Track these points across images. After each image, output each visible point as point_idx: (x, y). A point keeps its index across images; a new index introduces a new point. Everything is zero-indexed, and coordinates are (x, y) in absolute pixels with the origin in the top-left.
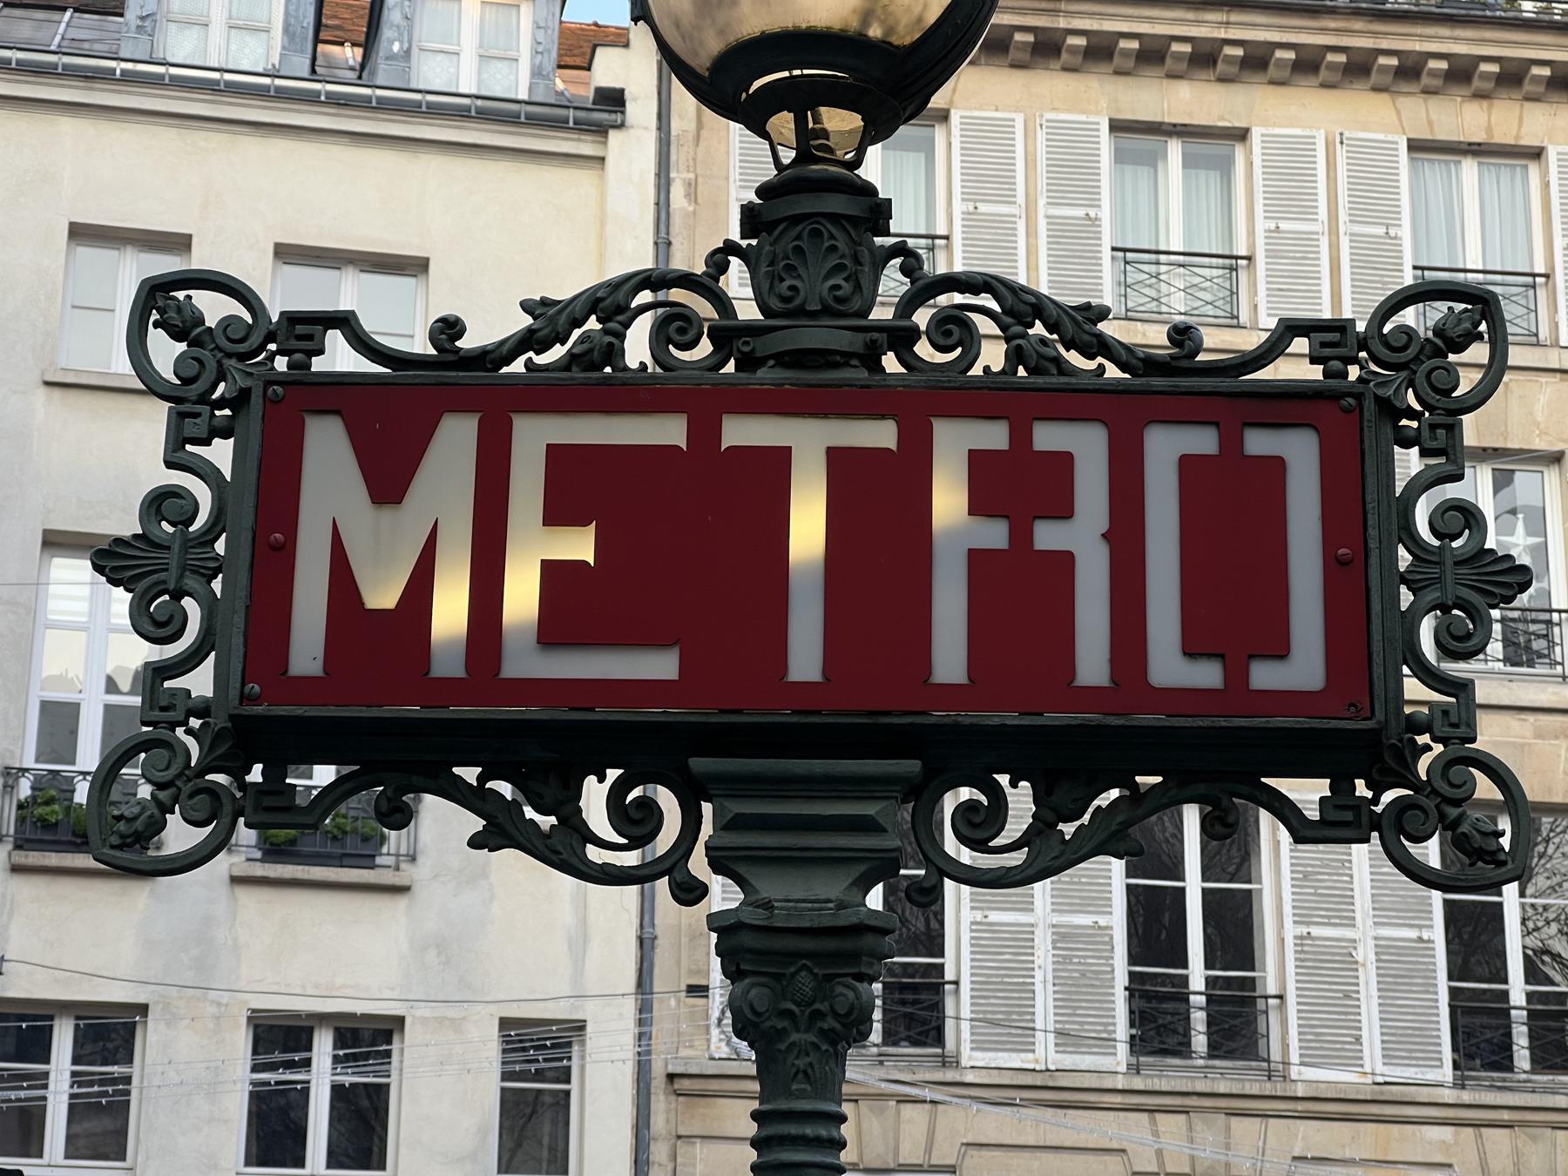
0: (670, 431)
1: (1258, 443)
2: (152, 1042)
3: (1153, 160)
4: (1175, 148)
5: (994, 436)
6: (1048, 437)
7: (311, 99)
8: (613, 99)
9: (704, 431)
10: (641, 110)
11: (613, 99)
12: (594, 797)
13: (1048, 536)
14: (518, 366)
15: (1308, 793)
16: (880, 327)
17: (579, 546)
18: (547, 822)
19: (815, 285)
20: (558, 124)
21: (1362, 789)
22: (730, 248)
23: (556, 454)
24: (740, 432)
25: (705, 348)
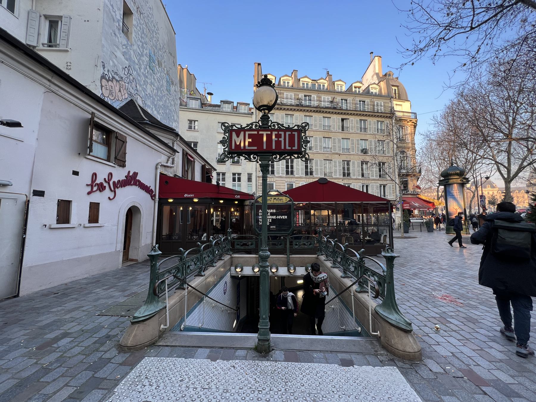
0: (256, 133)
1: (293, 133)
2: (226, 175)
3: (288, 117)
5: (276, 133)
6: (280, 133)
8: (252, 113)
9: (258, 133)
10: (254, 113)
11: (252, 113)
12: (252, 156)
13: (280, 139)
15: (296, 156)
17: (250, 140)
19: (265, 123)
24: (260, 133)
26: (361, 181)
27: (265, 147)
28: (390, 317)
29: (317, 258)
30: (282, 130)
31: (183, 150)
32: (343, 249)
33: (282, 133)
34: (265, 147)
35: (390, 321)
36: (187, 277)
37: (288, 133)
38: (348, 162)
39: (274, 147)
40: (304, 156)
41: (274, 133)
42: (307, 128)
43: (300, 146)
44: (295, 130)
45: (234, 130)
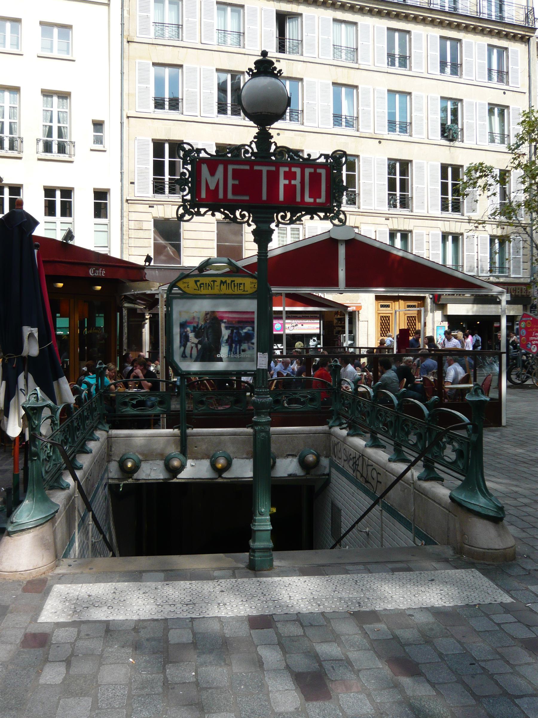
0: (247, 167)
1: (319, 171)
3: (225, 10)
4: (229, 9)
6: (293, 169)
9: (252, 168)
12: (238, 213)
15: (322, 215)
16: (272, 153)
17: (237, 182)
18: (232, 216)
21: (328, 214)
22: (253, 141)
23: (234, 170)
24: (256, 168)
25: (250, 155)
26: (440, 224)
29: (329, 434)
30: (298, 165)
32: (396, 401)
33: (298, 170)
35: (472, 507)
37: (308, 171)
38: (405, 165)
40: (337, 216)
41: (283, 170)
44: (321, 165)
45: (204, 160)
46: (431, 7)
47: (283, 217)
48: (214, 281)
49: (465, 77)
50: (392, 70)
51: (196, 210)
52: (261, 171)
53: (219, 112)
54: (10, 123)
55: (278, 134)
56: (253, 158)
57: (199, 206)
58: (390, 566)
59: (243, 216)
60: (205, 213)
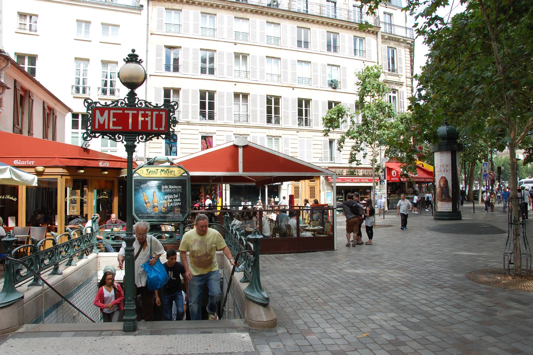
0: (121, 112)
1: (161, 113)
3: (206, 17)
4: (208, 16)
5: (143, 112)
6: (147, 112)
7: (105, 5)
9: (123, 112)
11: (142, 6)
13: (146, 119)
14: (111, 106)
17: (115, 120)
20: (135, 9)
24: (126, 112)
25: (124, 105)
27: (130, 128)
28: (252, 295)
31: (15, 81)
34: (130, 128)
36: (41, 273)
37: (155, 113)
38: (308, 102)
39: (140, 128)
41: (141, 113)
42: (176, 107)
43: (168, 126)
45: (98, 108)
46: (322, 15)
47: (142, 138)
48: (157, 170)
49: (340, 53)
50: (300, 49)
51: (94, 134)
52: (129, 114)
53: (202, 73)
54: (83, 79)
55: (235, 85)
56: (126, 106)
57: (96, 133)
58: (202, 330)
59: (119, 138)
60: (99, 136)
